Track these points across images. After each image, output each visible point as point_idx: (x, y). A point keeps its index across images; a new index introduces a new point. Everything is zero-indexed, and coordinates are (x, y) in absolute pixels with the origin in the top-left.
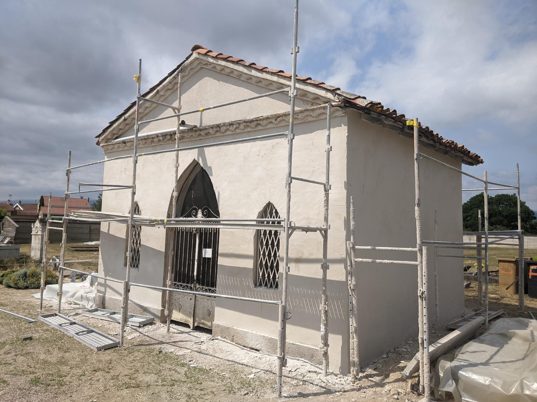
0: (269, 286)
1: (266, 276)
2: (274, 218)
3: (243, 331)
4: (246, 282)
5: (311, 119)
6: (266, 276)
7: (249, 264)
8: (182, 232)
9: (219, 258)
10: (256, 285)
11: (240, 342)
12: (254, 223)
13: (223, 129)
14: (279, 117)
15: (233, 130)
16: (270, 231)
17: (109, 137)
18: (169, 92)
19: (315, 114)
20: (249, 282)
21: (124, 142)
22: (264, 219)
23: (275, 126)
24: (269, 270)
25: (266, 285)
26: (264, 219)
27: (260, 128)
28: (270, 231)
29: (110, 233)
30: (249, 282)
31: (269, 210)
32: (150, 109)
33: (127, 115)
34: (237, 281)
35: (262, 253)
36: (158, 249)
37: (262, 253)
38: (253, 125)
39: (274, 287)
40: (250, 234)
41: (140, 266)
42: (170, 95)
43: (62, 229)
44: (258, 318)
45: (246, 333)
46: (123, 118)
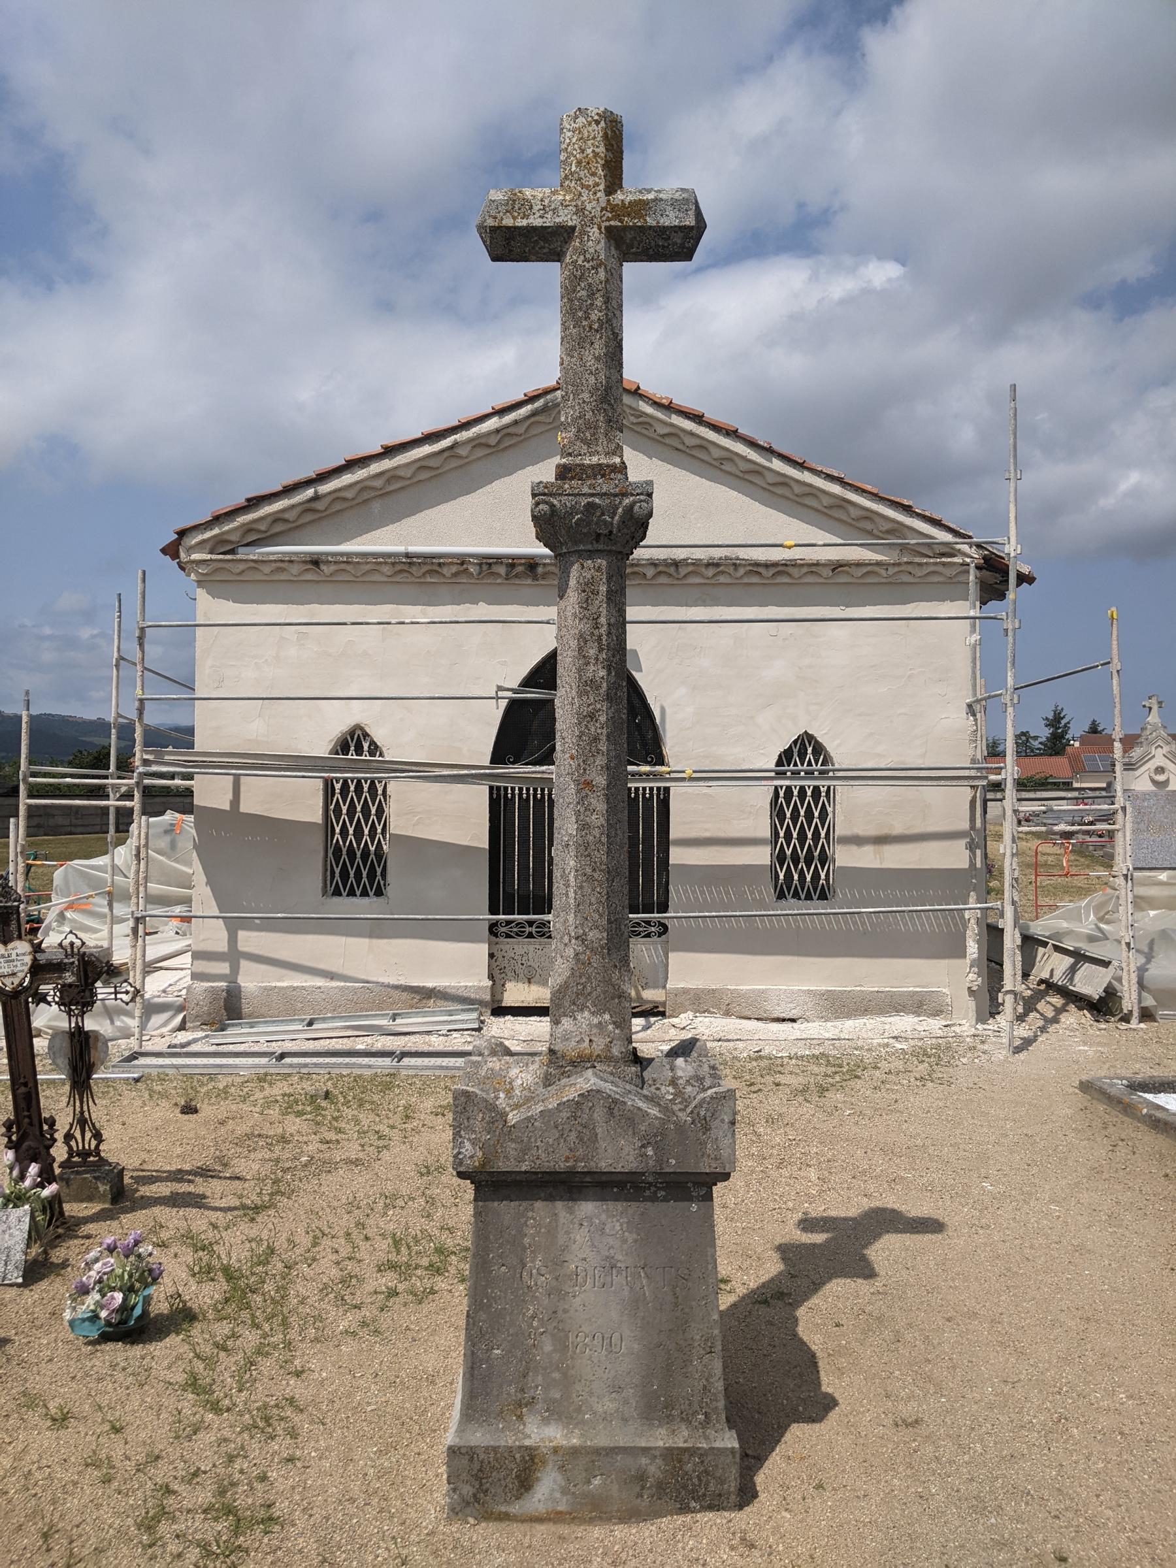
0: (803, 897)
1: (796, 877)
2: (795, 765)
3: (753, 991)
4: (752, 893)
5: (906, 578)
6: (796, 877)
7: (762, 856)
8: (524, 803)
9: (487, 847)
10: (324, 893)
11: (748, 1013)
12: (773, 774)
13: (683, 571)
14: (841, 566)
15: (420, 574)
16: (802, 790)
17: (234, 537)
18: (480, 452)
19: (919, 572)
20: (760, 893)
21: (315, 562)
22: (786, 768)
23: (386, 579)
24: (802, 864)
25: (796, 895)
26: (786, 768)
27: (786, 580)
28: (802, 790)
29: (244, 808)
30: (760, 893)
31: (804, 750)
32: (408, 482)
33: (324, 488)
34: (727, 893)
35: (338, 830)
36: (466, 843)
37: (338, 830)
38: (266, 569)
39: (371, 894)
40: (760, 796)
41: (390, 891)
42: (479, 459)
43: (132, 803)
44: (789, 958)
45: (764, 991)
46: (310, 492)
